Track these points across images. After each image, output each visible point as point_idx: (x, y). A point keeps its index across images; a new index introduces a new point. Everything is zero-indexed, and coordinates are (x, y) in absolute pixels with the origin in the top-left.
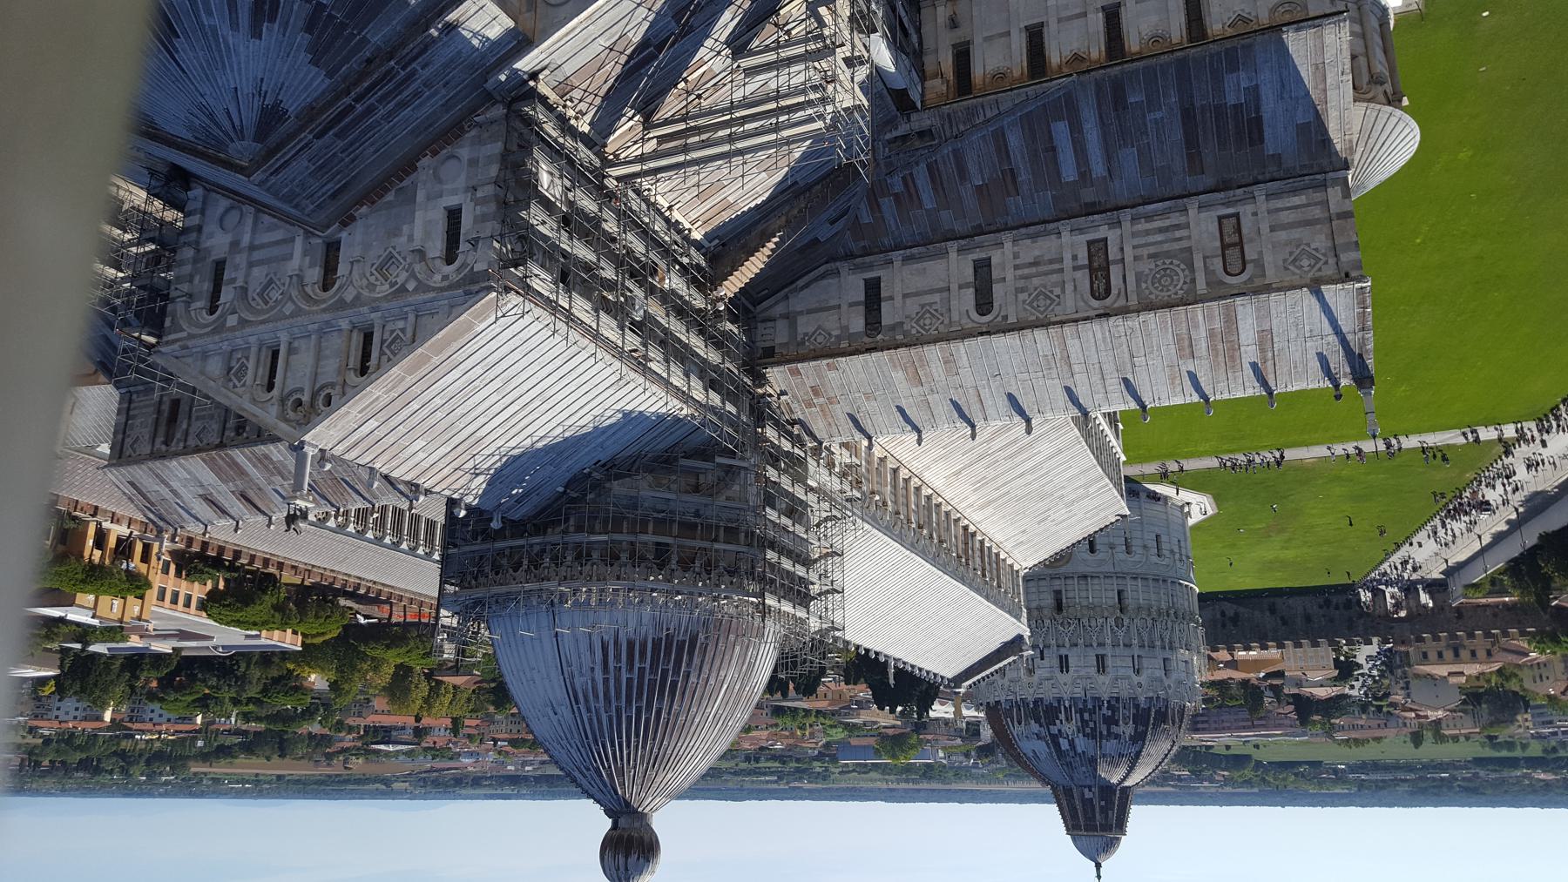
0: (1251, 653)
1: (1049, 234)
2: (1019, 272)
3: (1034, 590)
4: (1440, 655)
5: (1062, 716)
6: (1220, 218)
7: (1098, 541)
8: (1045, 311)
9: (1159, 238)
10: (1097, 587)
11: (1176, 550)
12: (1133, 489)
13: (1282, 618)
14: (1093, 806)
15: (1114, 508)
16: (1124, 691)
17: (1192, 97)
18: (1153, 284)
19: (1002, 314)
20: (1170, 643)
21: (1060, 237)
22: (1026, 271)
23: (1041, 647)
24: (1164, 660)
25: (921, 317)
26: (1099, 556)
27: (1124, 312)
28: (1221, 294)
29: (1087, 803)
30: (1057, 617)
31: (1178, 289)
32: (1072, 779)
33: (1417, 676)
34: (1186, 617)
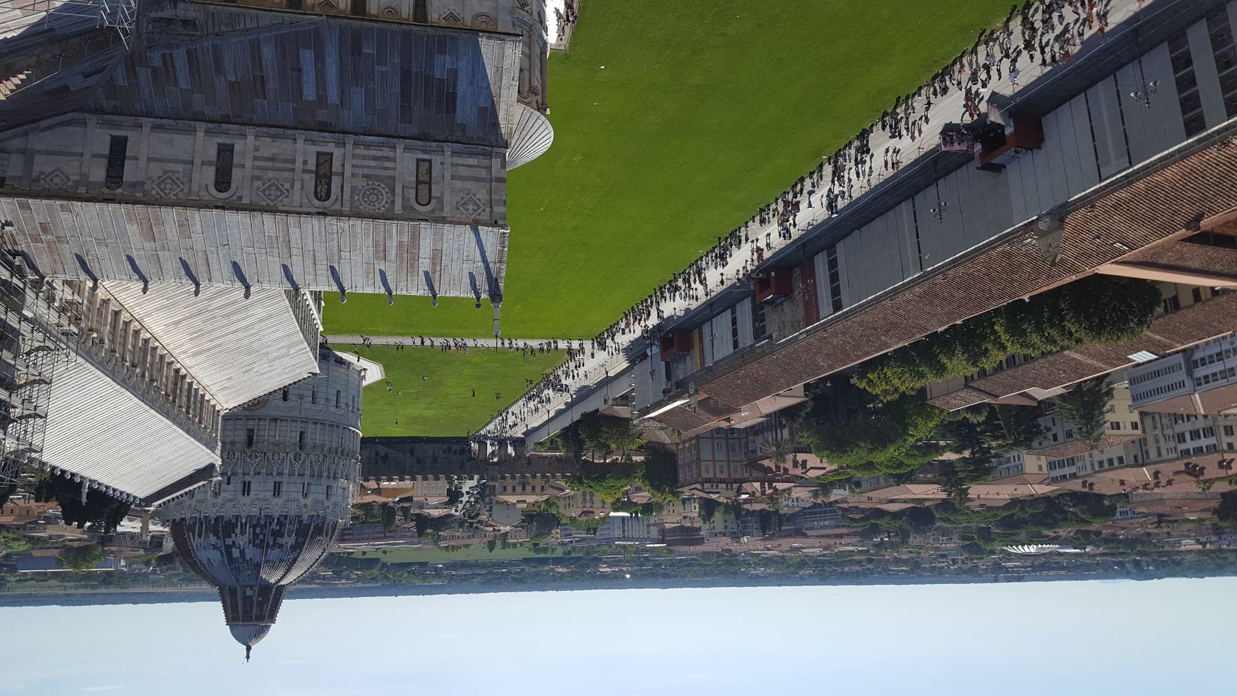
0: (392, 483)
1: (287, 137)
2: (258, 163)
3: (230, 427)
4: (514, 489)
6: (418, 160)
7: (290, 392)
8: (274, 200)
9: (373, 163)
10: (284, 428)
11: (351, 404)
12: (325, 354)
13: (417, 459)
14: (252, 601)
16: (292, 510)
17: (410, 63)
18: (363, 198)
19: (237, 194)
20: (335, 474)
21: (296, 143)
22: (264, 164)
23: (229, 474)
25: (163, 181)
26: (289, 404)
27: (339, 214)
30: (247, 450)
31: (381, 207)
32: (238, 580)
33: (498, 503)
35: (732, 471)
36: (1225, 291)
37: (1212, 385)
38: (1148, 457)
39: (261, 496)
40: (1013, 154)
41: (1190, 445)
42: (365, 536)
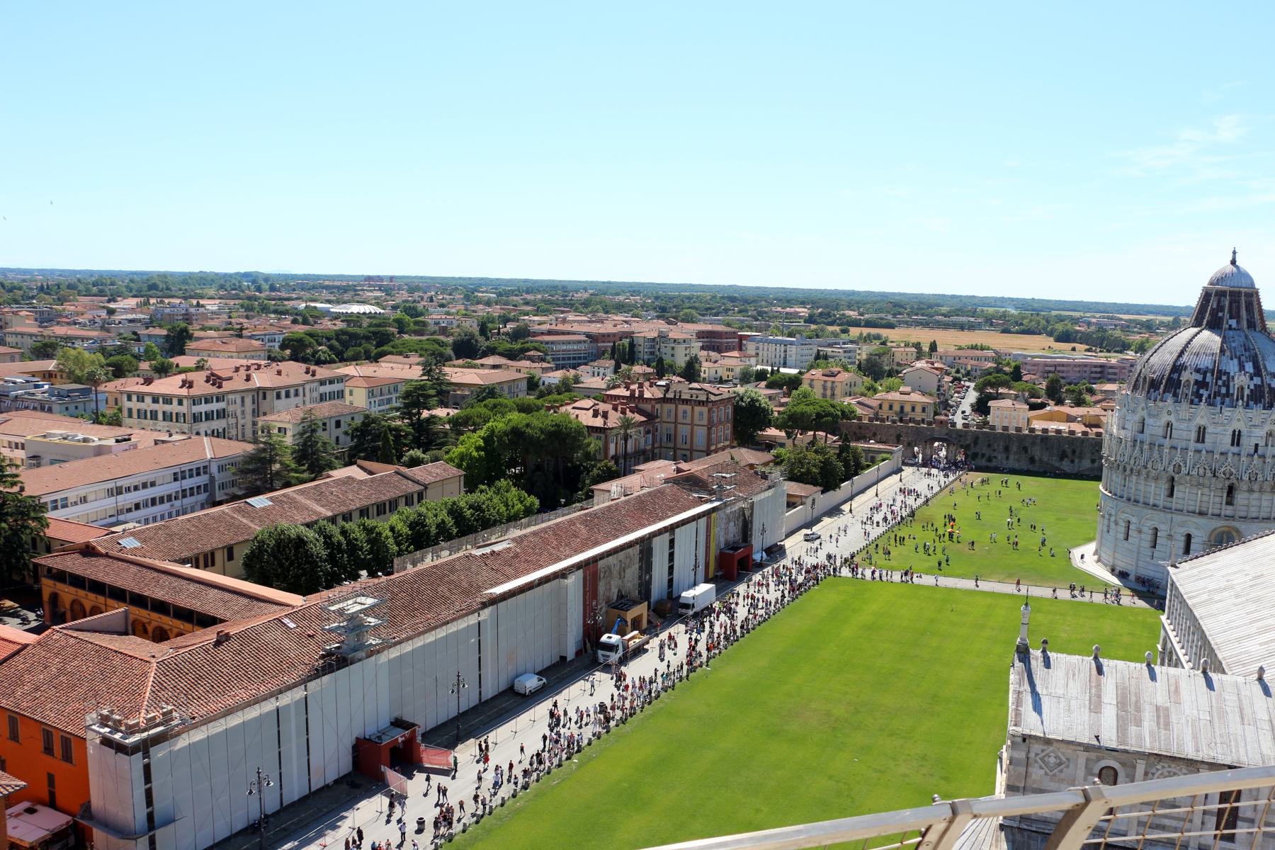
0: (1055, 427)
5: (1247, 392)
7: (1182, 544)
10: (1191, 503)
11: (1112, 525)
13: (1026, 452)
14: (1230, 311)
15: (1182, 575)
16: (1184, 408)
20: (1134, 446)
23: (1256, 456)
24: (1142, 432)
26: (1184, 531)
28: (1126, 755)
29: (1235, 314)
30: (1235, 481)
32: (1246, 337)
34: (1116, 466)
35: (673, 412)
36: (183, 562)
37: (194, 467)
38: (253, 396)
39: (1220, 429)
40: (383, 737)
41: (214, 406)
42: (1078, 369)
